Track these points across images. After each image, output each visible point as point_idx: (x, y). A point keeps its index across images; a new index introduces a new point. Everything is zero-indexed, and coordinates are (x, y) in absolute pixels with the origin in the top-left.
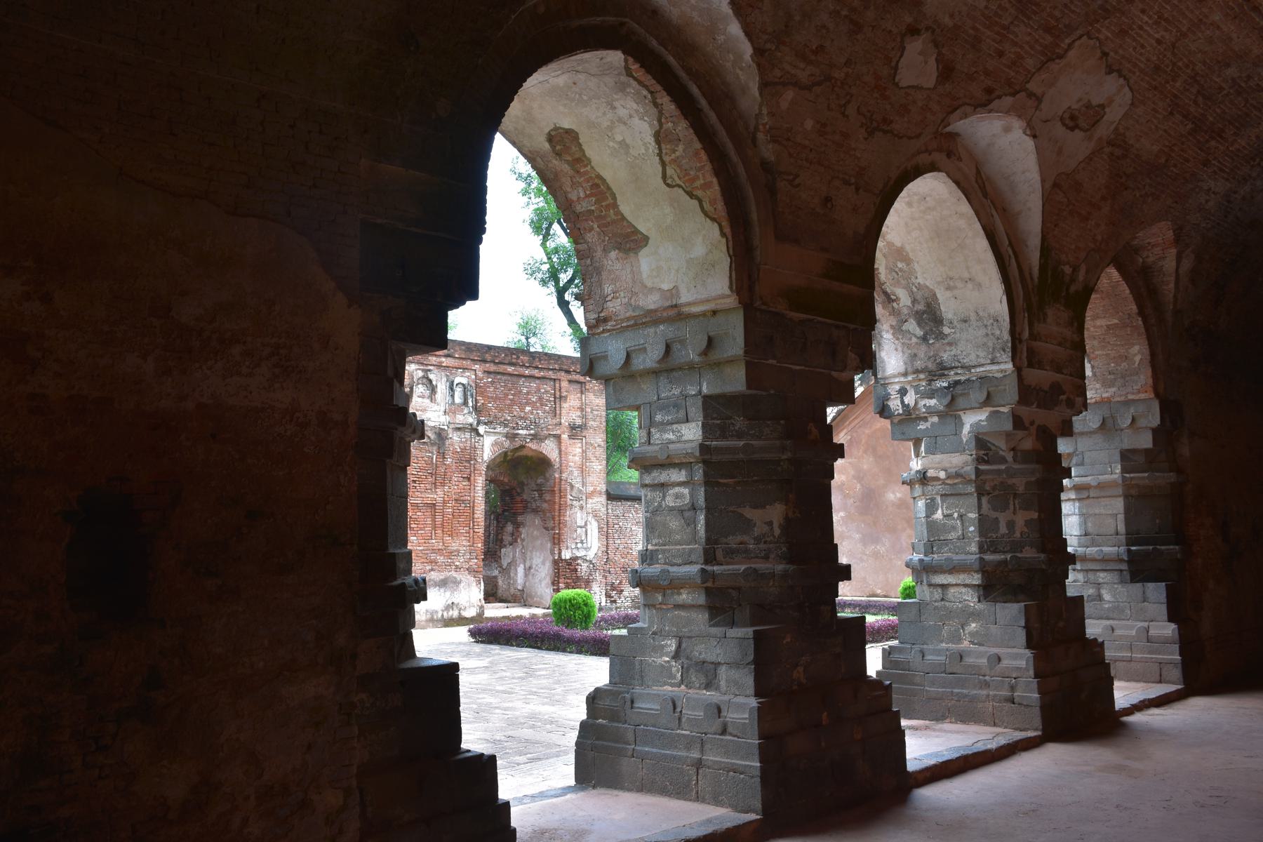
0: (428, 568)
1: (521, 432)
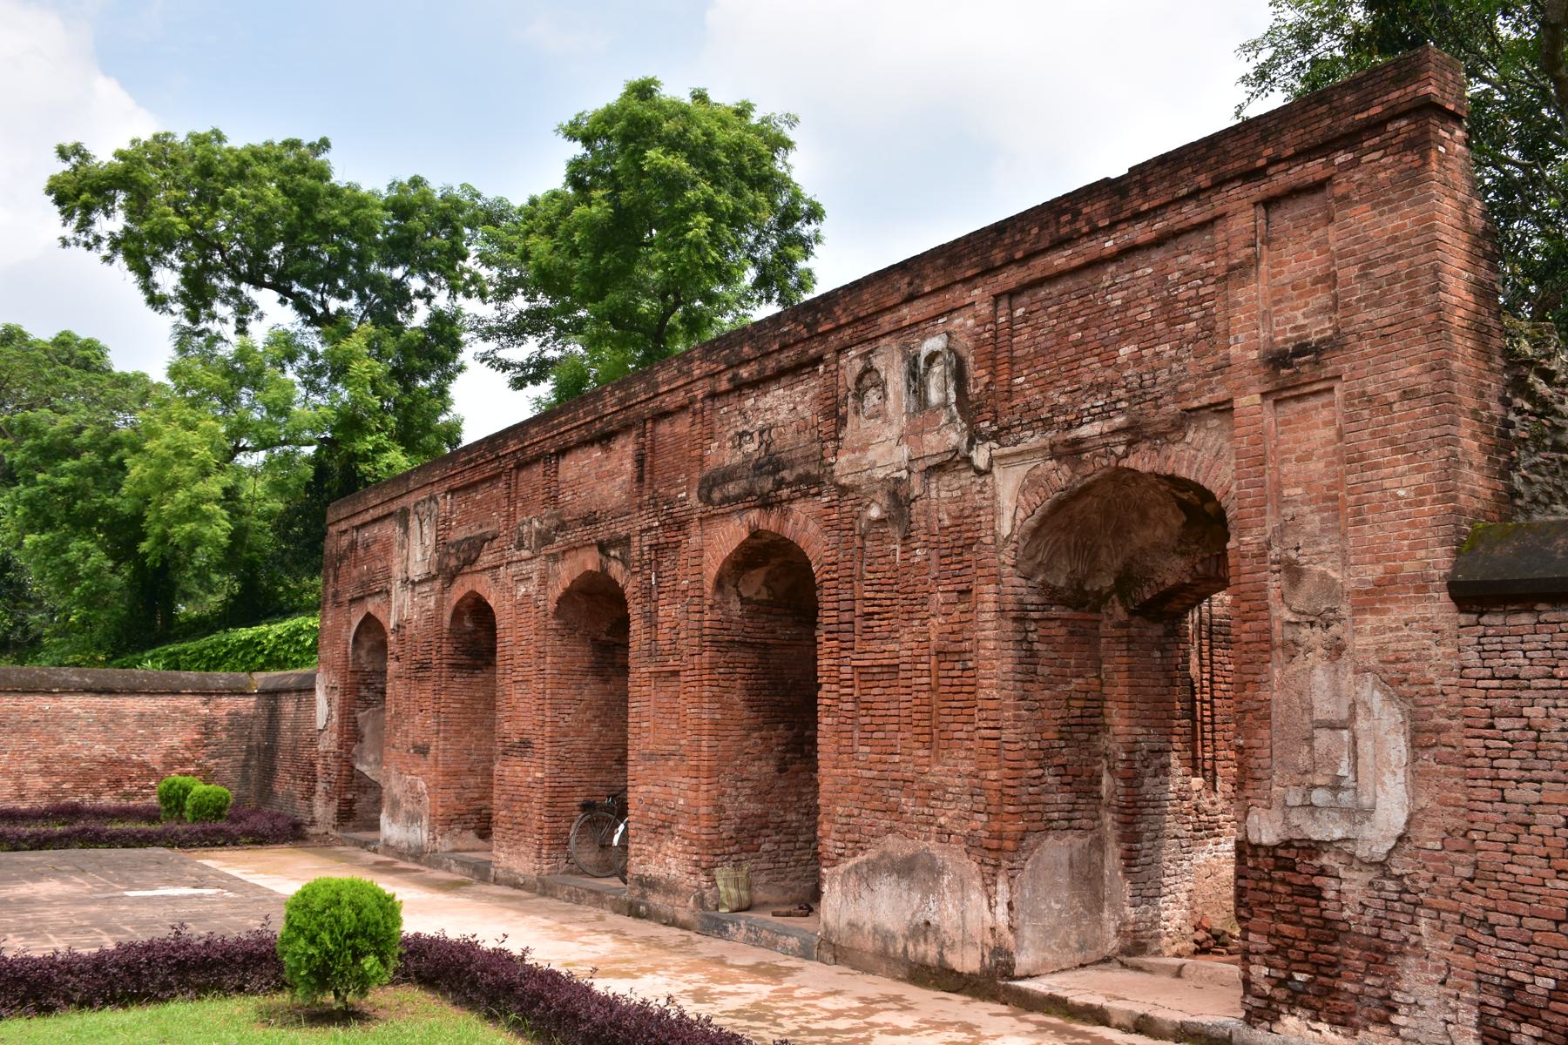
0: (885, 823)
1: (1085, 431)
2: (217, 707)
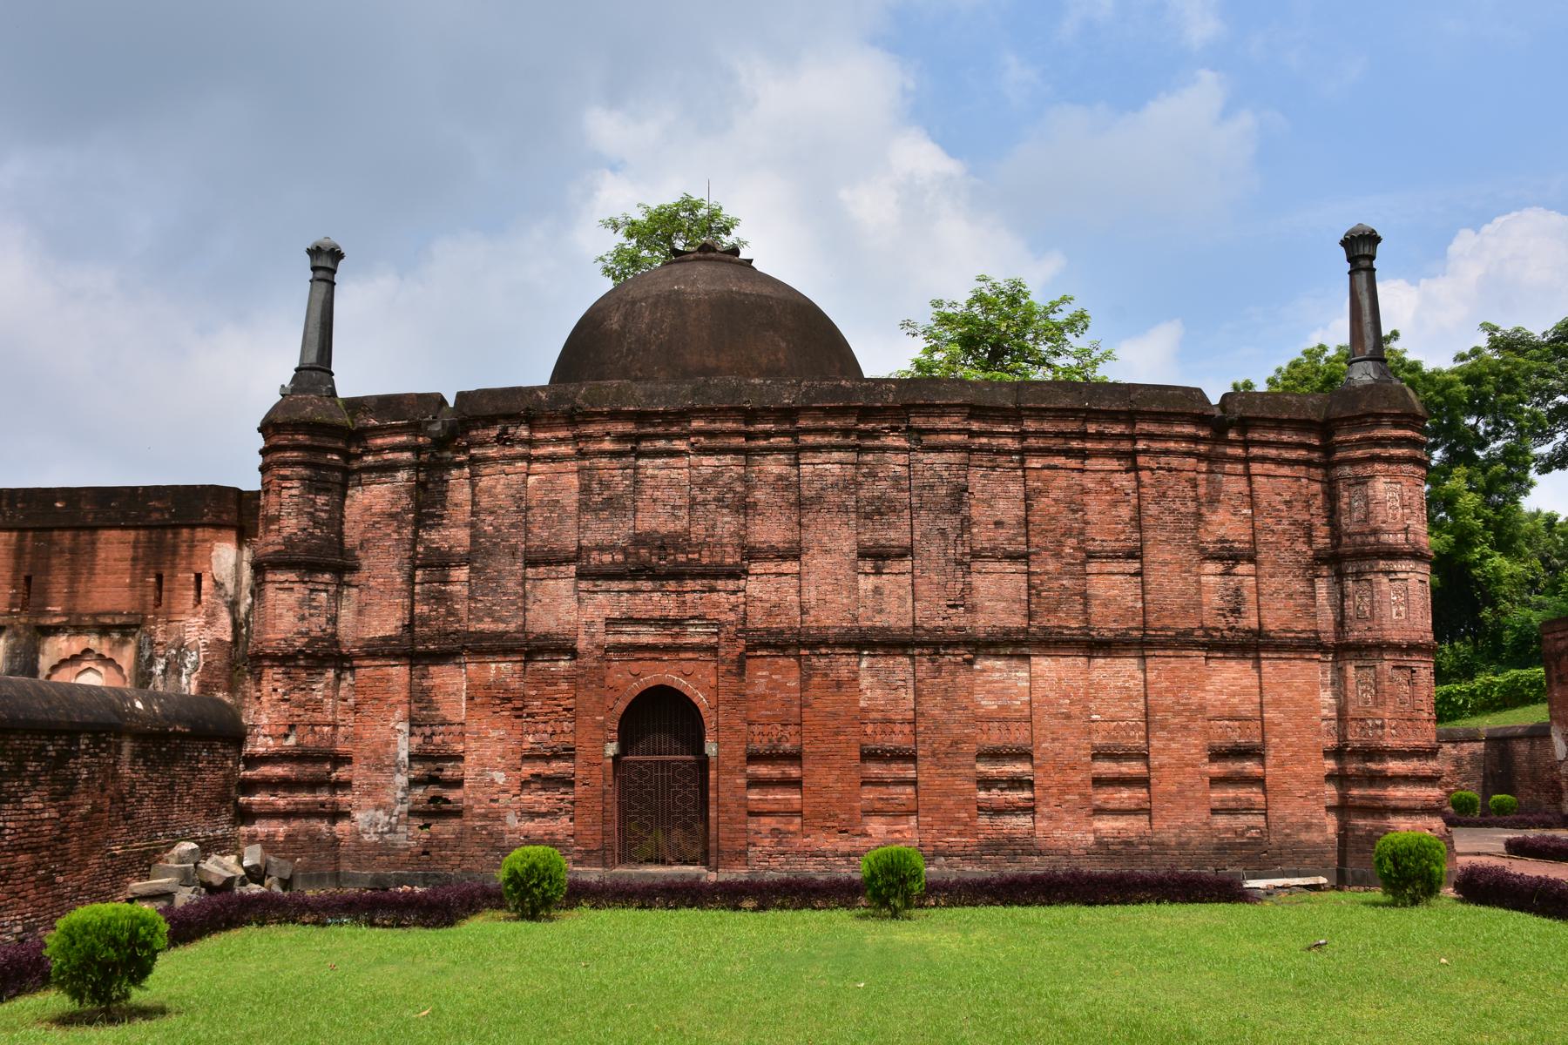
2: (1462, 749)
